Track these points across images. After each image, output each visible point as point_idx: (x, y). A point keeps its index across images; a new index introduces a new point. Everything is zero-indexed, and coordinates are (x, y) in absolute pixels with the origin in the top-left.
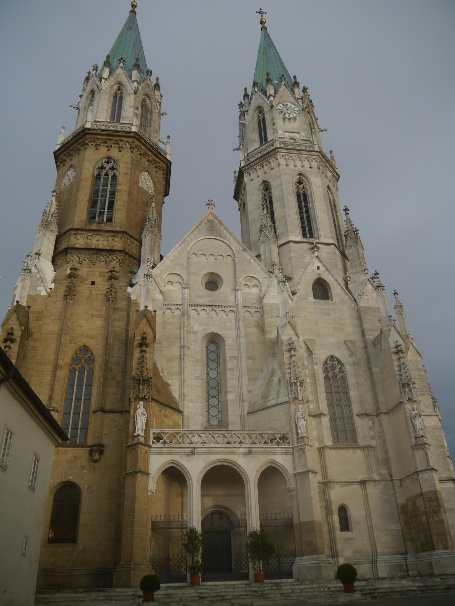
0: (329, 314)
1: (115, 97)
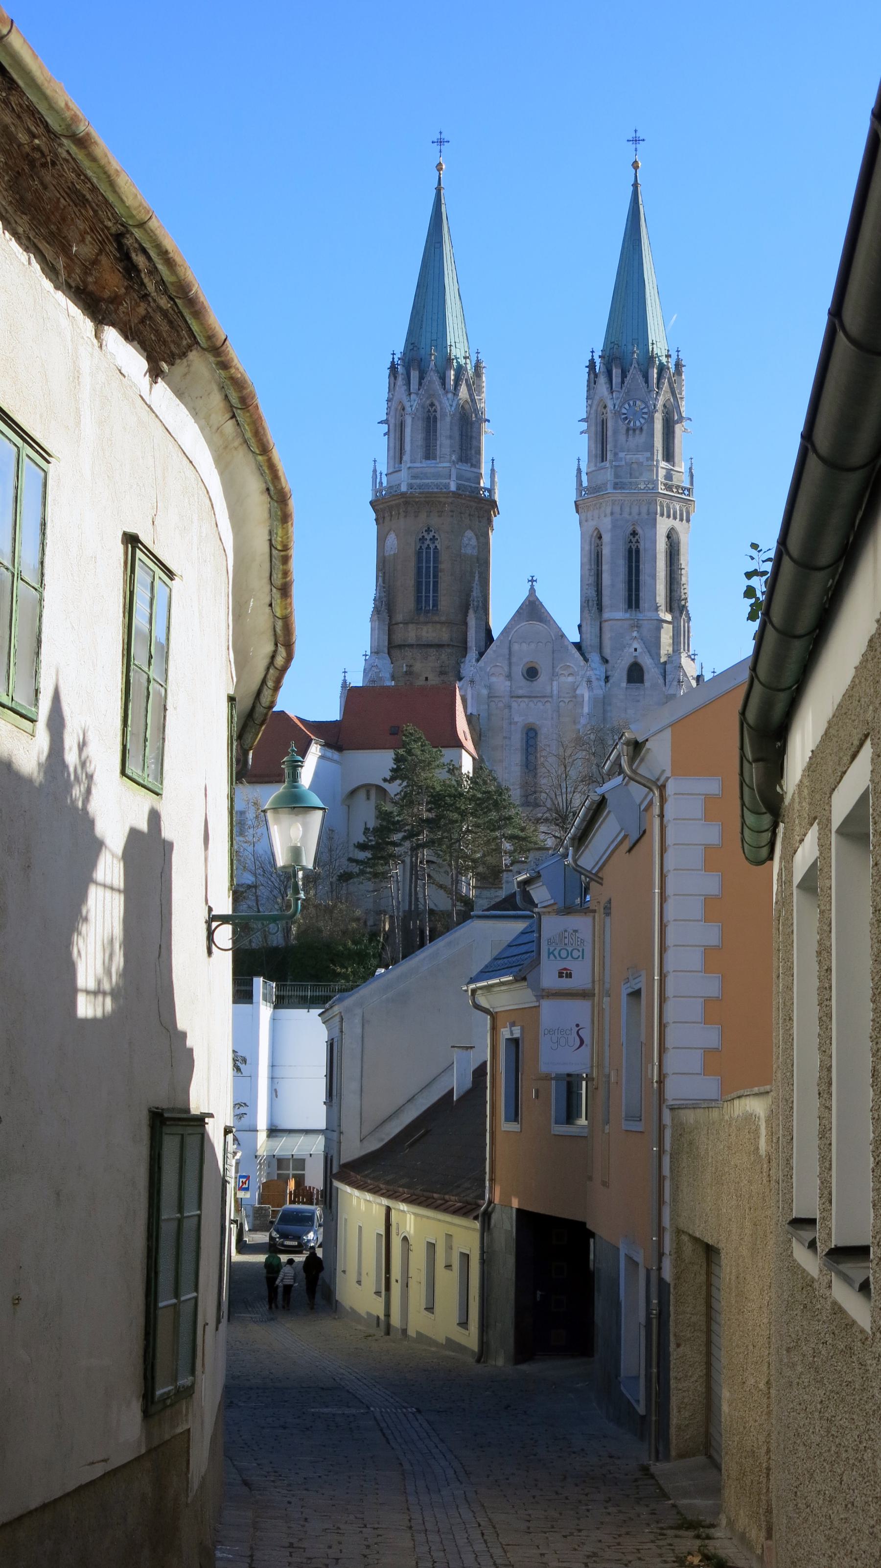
0: (638, 701)
1: (429, 418)
